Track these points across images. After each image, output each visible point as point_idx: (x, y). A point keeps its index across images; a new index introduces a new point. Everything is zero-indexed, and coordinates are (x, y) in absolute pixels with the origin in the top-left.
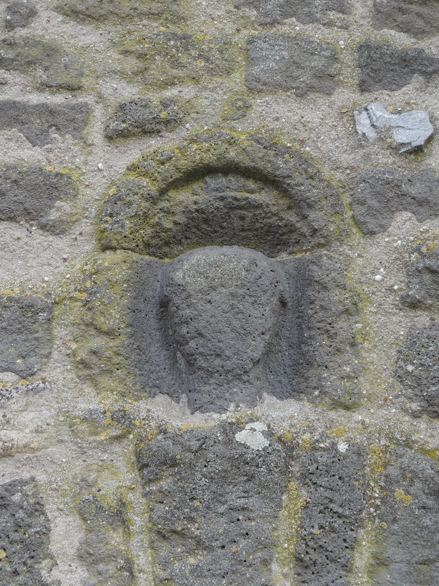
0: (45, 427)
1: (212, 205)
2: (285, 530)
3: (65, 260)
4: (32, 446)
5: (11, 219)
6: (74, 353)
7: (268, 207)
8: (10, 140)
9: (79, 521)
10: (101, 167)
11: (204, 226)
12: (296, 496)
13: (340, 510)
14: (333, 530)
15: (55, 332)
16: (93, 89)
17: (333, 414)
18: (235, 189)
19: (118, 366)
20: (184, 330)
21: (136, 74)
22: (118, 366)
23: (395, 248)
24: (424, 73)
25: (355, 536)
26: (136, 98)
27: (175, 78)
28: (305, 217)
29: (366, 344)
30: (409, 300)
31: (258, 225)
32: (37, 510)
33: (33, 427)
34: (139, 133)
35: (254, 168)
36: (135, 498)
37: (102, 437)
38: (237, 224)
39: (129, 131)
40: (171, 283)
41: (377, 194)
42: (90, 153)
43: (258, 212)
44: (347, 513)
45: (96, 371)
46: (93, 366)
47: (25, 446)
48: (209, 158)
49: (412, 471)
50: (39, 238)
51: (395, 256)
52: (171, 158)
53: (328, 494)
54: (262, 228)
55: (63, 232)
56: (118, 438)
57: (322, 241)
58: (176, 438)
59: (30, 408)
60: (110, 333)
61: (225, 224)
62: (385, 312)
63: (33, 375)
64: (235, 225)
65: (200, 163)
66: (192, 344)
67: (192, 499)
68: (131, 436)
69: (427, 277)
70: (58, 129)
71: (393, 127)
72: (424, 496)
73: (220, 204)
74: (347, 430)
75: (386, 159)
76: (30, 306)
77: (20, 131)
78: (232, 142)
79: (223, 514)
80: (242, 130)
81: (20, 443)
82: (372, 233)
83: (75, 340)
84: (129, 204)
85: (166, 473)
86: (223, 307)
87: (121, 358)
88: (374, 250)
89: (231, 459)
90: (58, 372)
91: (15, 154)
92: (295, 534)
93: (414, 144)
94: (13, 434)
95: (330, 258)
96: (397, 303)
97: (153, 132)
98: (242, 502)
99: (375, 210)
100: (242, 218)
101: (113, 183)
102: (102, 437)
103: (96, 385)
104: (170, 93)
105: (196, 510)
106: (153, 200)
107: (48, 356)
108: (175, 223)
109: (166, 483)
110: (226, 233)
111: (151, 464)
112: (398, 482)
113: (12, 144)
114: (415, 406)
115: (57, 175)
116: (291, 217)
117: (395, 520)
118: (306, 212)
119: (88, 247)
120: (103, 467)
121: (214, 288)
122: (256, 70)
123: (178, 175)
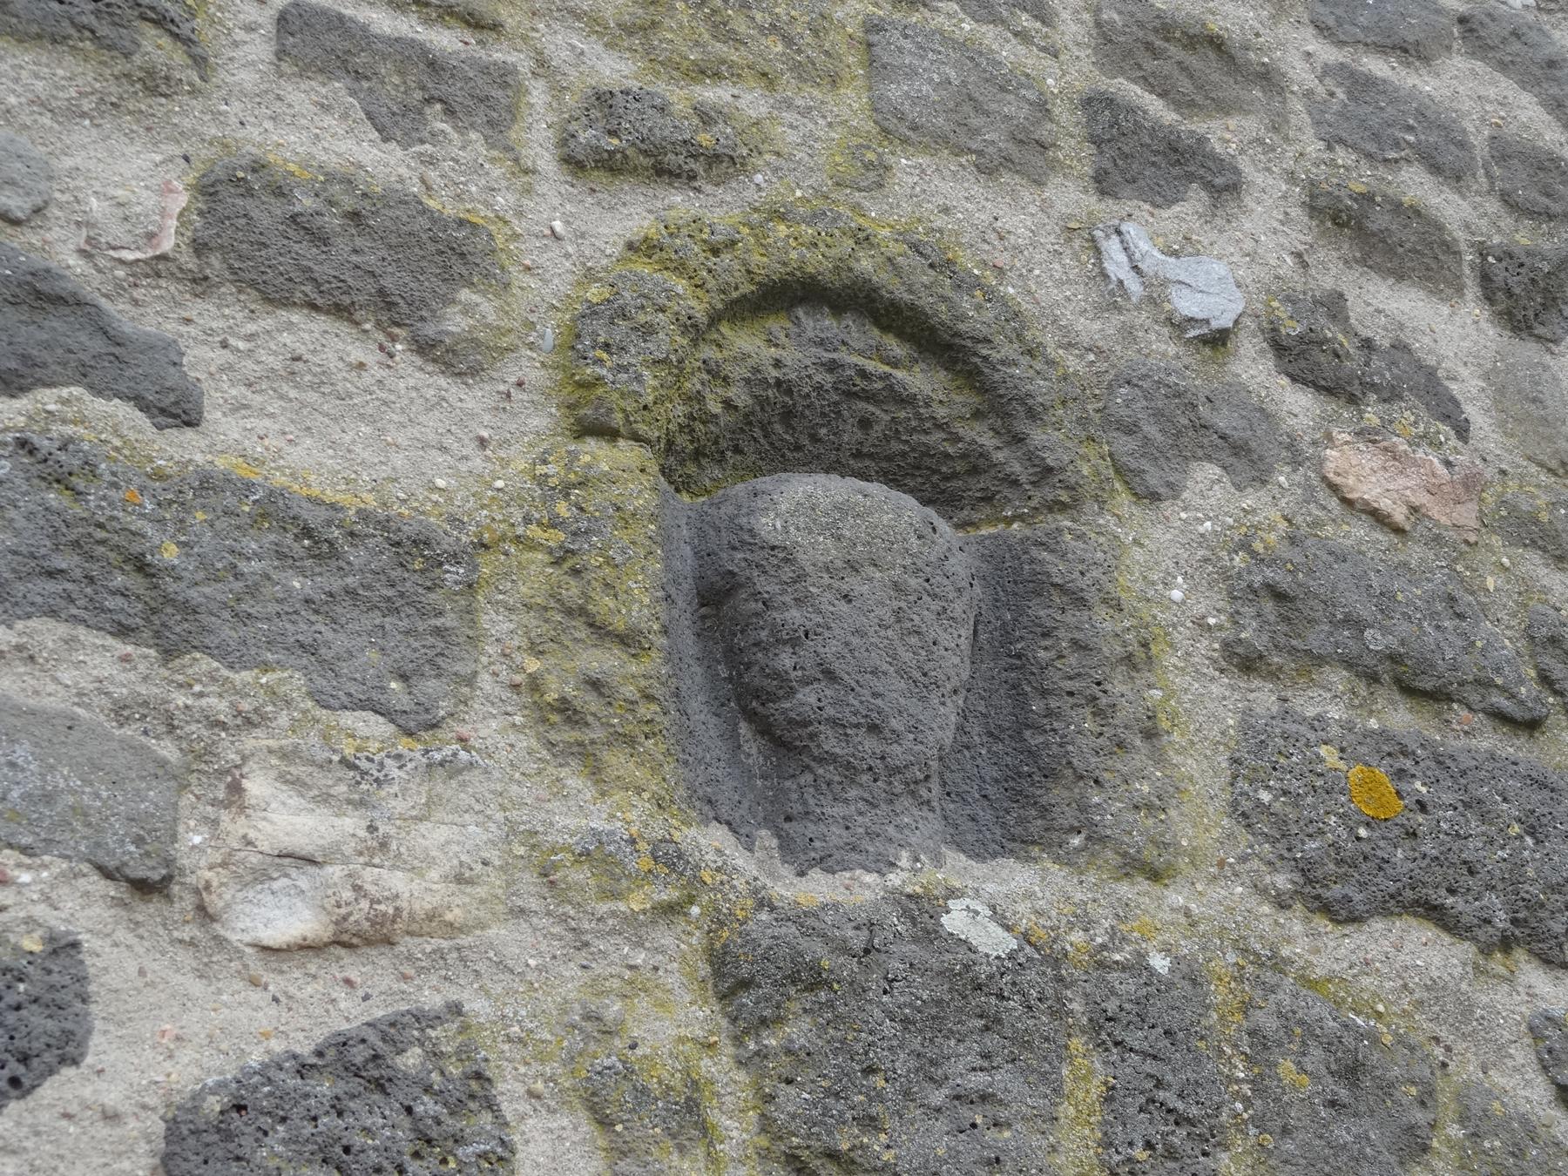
0: (478, 867)
1: (809, 377)
3: (482, 443)
4: (449, 917)
5: (341, 311)
6: (535, 684)
7: (927, 405)
8: (326, 108)
9: (587, 1127)
11: (778, 428)
13: (1180, 1105)
14: (1171, 1154)
15: (484, 621)
16: (524, 38)
17: (1124, 889)
18: (860, 347)
19: (646, 729)
20: (785, 660)
21: (629, 30)
22: (646, 729)
23: (1202, 535)
24: (1208, 186)
25: (1213, 1166)
26: (634, 85)
27: (723, 62)
28: (1018, 439)
29: (1176, 736)
30: (1240, 650)
31: (896, 446)
32: (472, 1097)
33: (447, 866)
34: (647, 169)
35: (912, 307)
36: (719, 1068)
37: (637, 903)
38: (851, 435)
39: (626, 157)
40: (747, 540)
41: (1158, 415)
42: (528, 191)
43: (902, 414)
44: (1194, 1111)
45: (598, 734)
46: (590, 719)
47: (430, 917)
48: (817, 262)
49: (1301, 1023)
50: (412, 377)
51: (1201, 553)
52: (734, 243)
53: (1150, 1067)
54: (904, 454)
55: (475, 371)
56: (671, 910)
57: (1064, 497)
58: (802, 918)
59: (439, 814)
60: (628, 640)
61: (823, 431)
62: (1197, 671)
63: (434, 726)
64: (846, 438)
65: (800, 268)
66: (807, 697)
67: (870, 1071)
68: (695, 910)
69: (1269, 606)
70: (450, 112)
71: (1170, 281)
72: (1330, 1080)
73: (822, 377)
75: (1162, 347)
76: (421, 543)
77: (353, 93)
78: (864, 240)
79: (938, 1110)
80: (884, 215)
81: (417, 906)
82: (1155, 497)
83: (535, 650)
84: (648, 331)
85: (795, 1007)
86: (879, 611)
87: (655, 707)
88: (1160, 535)
89: (945, 973)
91: (342, 147)
92: (1096, 1161)
93: (1215, 325)
94: (397, 881)
95: (1080, 537)
96: (1216, 655)
97: (678, 176)
98: (978, 1080)
99: (1157, 448)
100: (865, 423)
101: (590, 276)
102: (637, 903)
103: (595, 772)
104: (714, 94)
105: (880, 1097)
106: (695, 331)
107: (470, 680)
108: (728, 404)
109: (799, 1031)
110: (818, 457)
112: (1280, 1045)
113: (328, 121)
114: (1282, 881)
115: (461, 223)
116: (982, 436)
117: (1285, 1131)
118: (1022, 425)
119: (538, 422)
120: (636, 985)
121: (853, 567)
122: (895, 92)
123: (747, 288)
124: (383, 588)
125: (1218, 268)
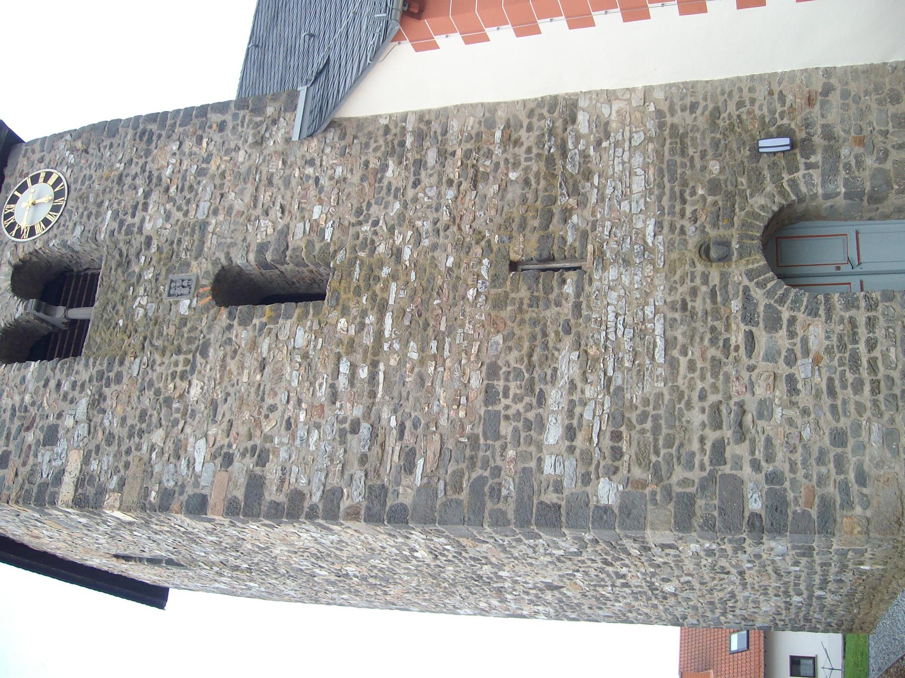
2: (749, 242)
10: (700, 267)
12: (744, 241)
18: (702, 251)
74: (736, 236)
90: (730, 270)
111: (741, 257)
124: (724, 276)
125: (690, 229)
